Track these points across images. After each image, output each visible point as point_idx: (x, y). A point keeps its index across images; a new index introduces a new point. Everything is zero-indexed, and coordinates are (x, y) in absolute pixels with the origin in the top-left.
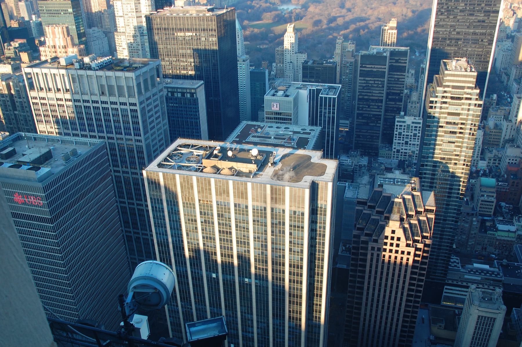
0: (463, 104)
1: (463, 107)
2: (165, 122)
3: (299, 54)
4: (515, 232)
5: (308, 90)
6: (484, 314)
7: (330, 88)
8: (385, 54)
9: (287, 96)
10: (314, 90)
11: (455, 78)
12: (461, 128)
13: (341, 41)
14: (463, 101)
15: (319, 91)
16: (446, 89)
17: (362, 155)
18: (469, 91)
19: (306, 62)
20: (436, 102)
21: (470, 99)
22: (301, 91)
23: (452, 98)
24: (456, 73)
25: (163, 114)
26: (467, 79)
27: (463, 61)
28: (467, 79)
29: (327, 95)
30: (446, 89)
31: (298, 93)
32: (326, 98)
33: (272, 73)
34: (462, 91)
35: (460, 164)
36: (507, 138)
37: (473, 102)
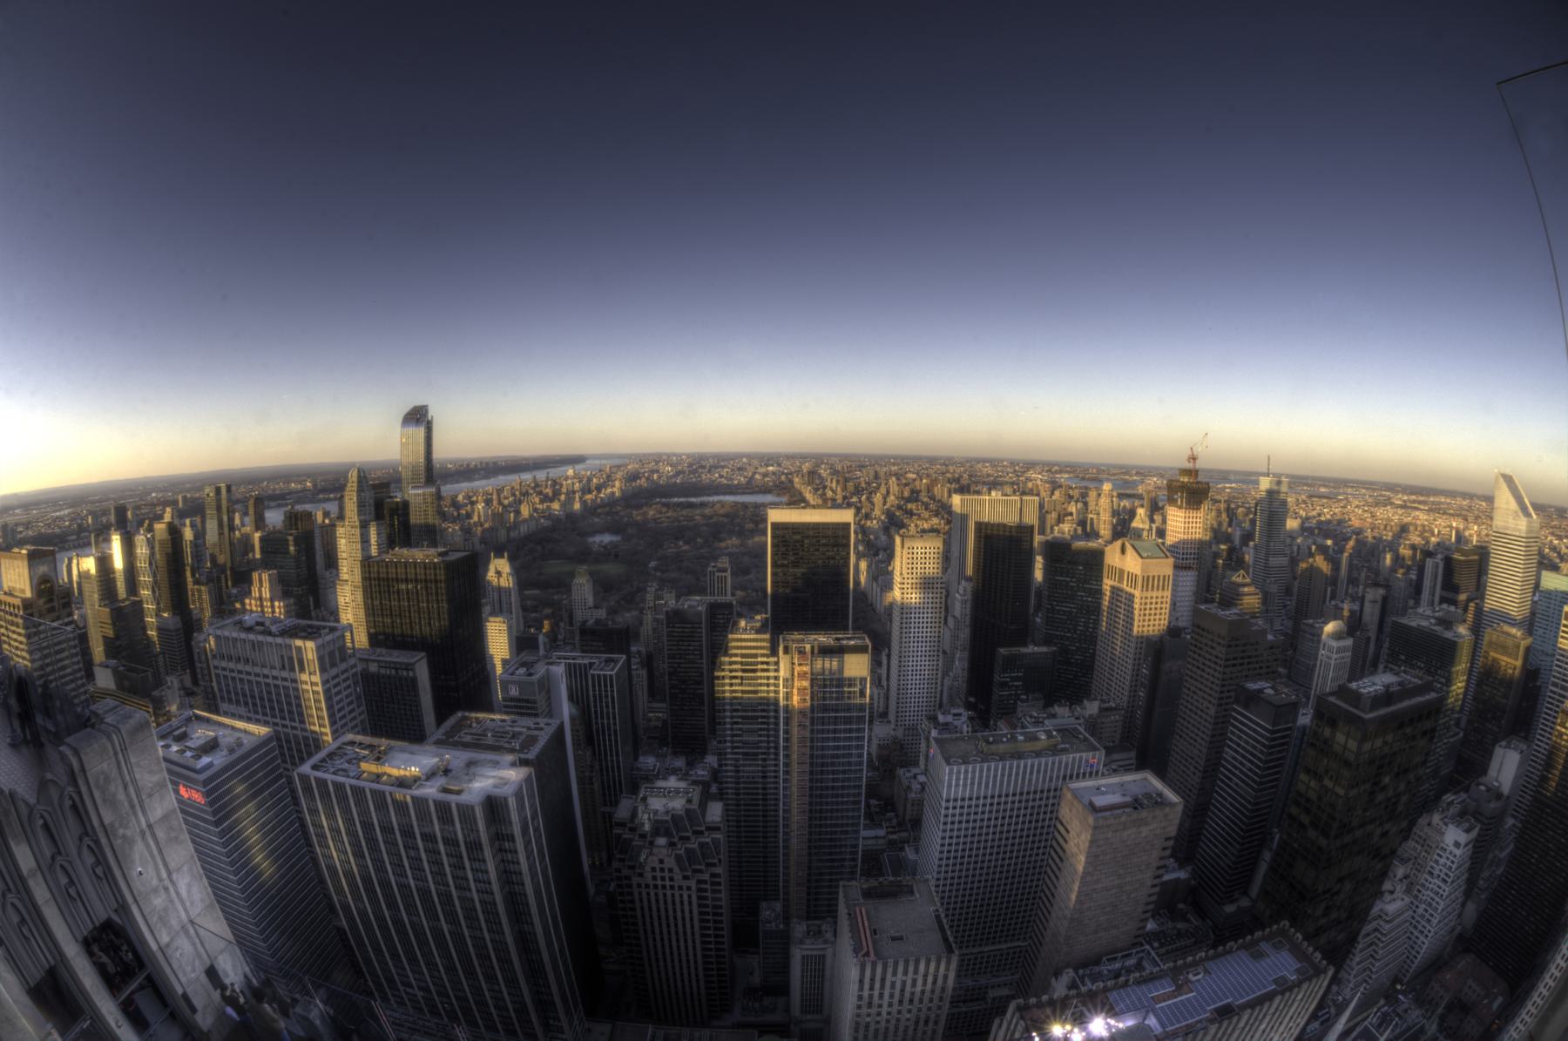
0: (761, 678)
1: (759, 681)
2: (362, 708)
3: (593, 610)
4: (884, 837)
5: (563, 665)
6: (808, 953)
7: (608, 661)
8: (700, 608)
9: (530, 675)
10: (585, 664)
12: (763, 711)
13: (653, 589)
14: (759, 674)
15: (591, 665)
16: (734, 659)
17: (675, 754)
18: (765, 659)
19: (586, 621)
20: (723, 678)
21: (767, 670)
22: (551, 667)
23: (744, 671)
24: (743, 637)
25: (358, 698)
26: (759, 644)
28: (759, 644)
29: (602, 670)
30: (734, 659)
31: (548, 669)
32: (599, 676)
33: (560, 637)
35: (771, 760)
36: (881, 710)
37: (772, 674)
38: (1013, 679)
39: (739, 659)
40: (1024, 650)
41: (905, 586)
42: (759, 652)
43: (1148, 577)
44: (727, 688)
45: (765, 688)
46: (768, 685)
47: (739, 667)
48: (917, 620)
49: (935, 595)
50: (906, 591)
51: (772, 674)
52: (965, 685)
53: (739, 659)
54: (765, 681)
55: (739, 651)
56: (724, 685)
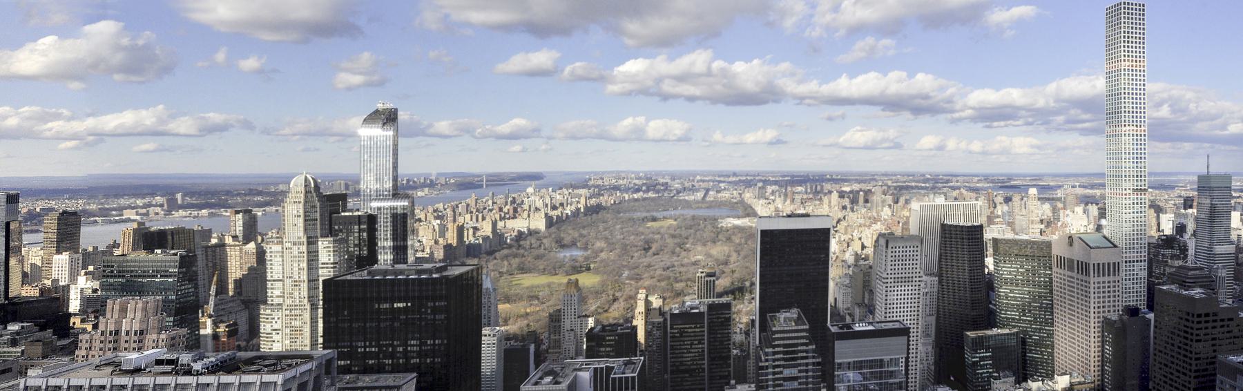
0: (800, 365)
1: (799, 368)
11: (785, 335)
14: (799, 361)
16: (776, 349)
18: (805, 348)
20: (767, 367)
21: (806, 358)
24: (786, 329)
26: (800, 334)
27: (794, 313)
28: (800, 334)
30: (776, 349)
34: (796, 349)
37: (811, 361)
38: (982, 359)
39: (782, 349)
40: (989, 332)
41: (889, 281)
42: (799, 341)
43: (1098, 264)
44: (770, 377)
45: (804, 374)
46: (807, 371)
47: (781, 356)
48: (898, 310)
49: (914, 288)
50: (889, 285)
51: (811, 361)
52: (933, 368)
53: (782, 349)
54: (804, 368)
55: (782, 342)
56: (767, 374)
